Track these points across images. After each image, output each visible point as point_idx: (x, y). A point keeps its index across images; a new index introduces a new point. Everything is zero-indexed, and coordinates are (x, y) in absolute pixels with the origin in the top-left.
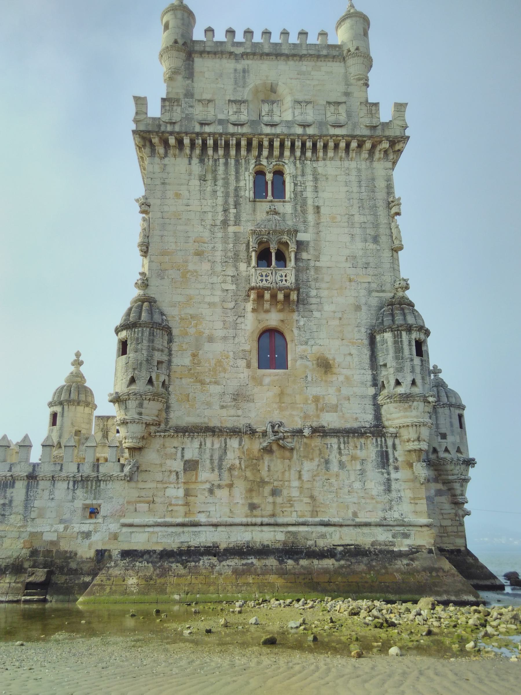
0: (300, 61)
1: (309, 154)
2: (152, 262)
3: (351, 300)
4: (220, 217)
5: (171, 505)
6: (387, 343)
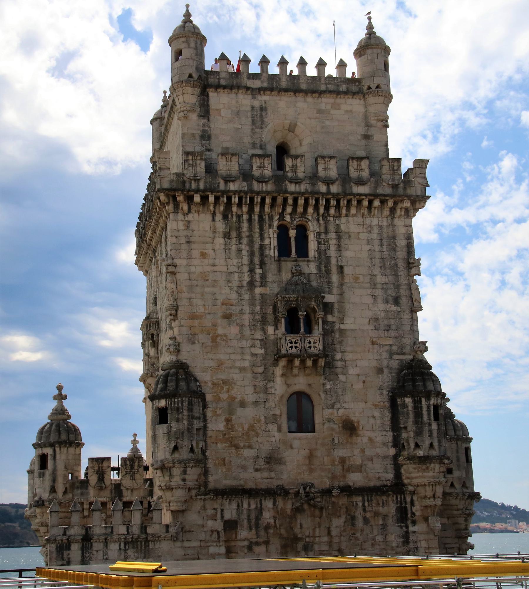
2: (182, 326)
3: (375, 364)
6: (407, 407)
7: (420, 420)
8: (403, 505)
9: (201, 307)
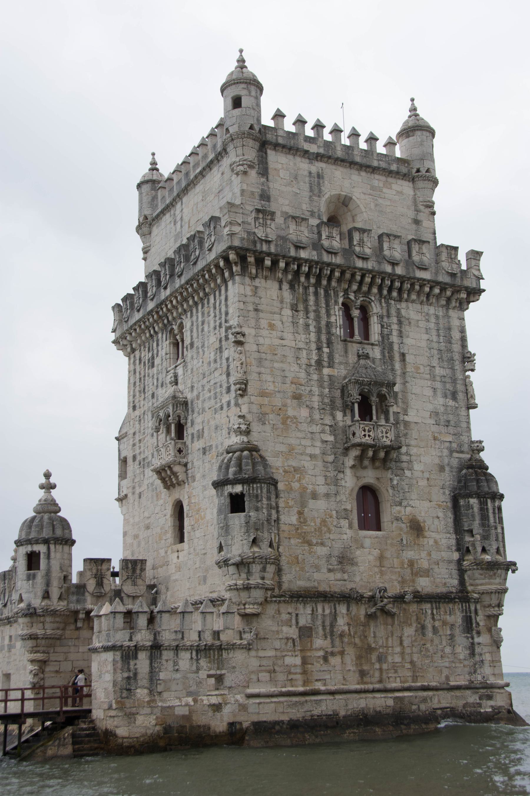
0: (371, 173)
1: (395, 294)
2: (252, 403)
3: (437, 461)
4: (315, 357)
5: (290, 673)
6: (472, 509)
7: (487, 522)
8: (468, 614)
9: (270, 384)
